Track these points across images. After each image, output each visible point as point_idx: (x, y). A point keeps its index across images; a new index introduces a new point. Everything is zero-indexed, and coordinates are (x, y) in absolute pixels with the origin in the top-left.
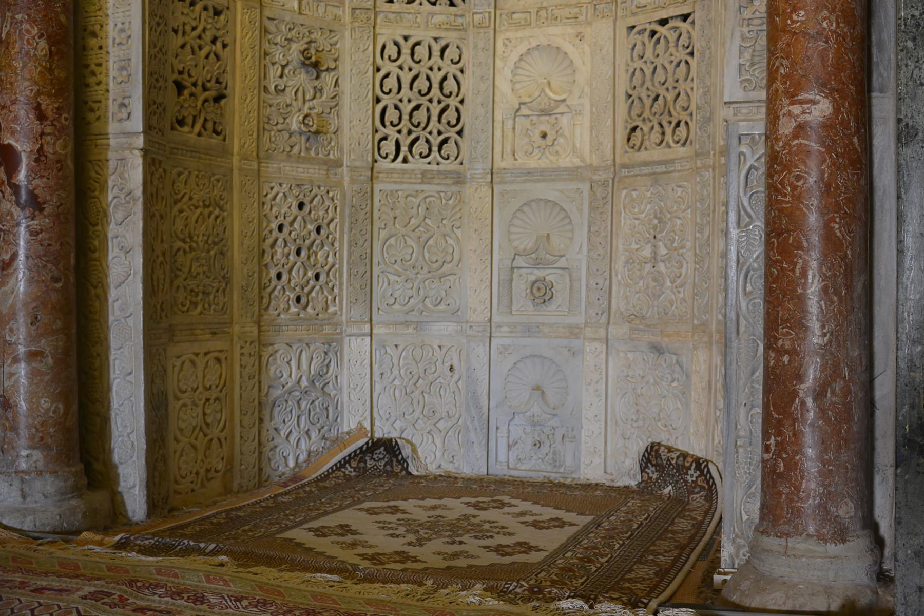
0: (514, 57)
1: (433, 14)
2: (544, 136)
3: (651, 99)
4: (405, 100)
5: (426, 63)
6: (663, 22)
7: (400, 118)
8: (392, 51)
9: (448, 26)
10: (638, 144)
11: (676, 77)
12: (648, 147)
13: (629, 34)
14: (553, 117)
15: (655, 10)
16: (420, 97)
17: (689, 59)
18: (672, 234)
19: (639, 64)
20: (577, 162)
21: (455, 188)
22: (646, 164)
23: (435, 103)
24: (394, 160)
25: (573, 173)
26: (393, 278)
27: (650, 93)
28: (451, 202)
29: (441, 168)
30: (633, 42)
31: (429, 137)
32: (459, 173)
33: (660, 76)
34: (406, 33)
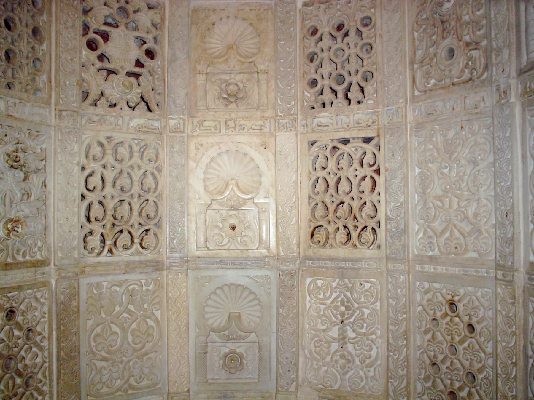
0: (205, 160)
1: (131, 119)
2: (234, 228)
3: (335, 205)
4: (109, 197)
5: (127, 164)
6: (346, 142)
7: (105, 215)
8: (97, 150)
9: (146, 129)
10: (323, 241)
11: (361, 189)
12: (334, 244)
13: (309, 149)
14: (241, 212)
15: (337, 130)
16: (122, 194)
17: (375, 176)
18: (361, 322)
19: (321, 174)
20: (264, 252)
21: (154, 275)
22: (331, 259)
23: (136, 200)
24: (99, 254)
25: (260, 262)
26: (100, 364)
27: (334, 199)
28: (150, 288)
29: (143, 258)
30: (315, 154)
31: (131, 230)
32: (158, 262)
33: (344, 186)
34: (109, 134)
